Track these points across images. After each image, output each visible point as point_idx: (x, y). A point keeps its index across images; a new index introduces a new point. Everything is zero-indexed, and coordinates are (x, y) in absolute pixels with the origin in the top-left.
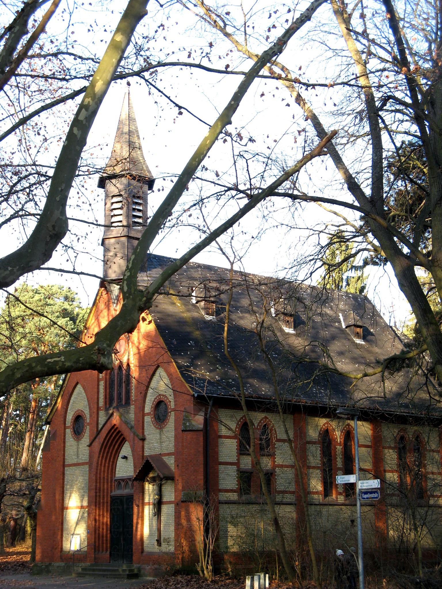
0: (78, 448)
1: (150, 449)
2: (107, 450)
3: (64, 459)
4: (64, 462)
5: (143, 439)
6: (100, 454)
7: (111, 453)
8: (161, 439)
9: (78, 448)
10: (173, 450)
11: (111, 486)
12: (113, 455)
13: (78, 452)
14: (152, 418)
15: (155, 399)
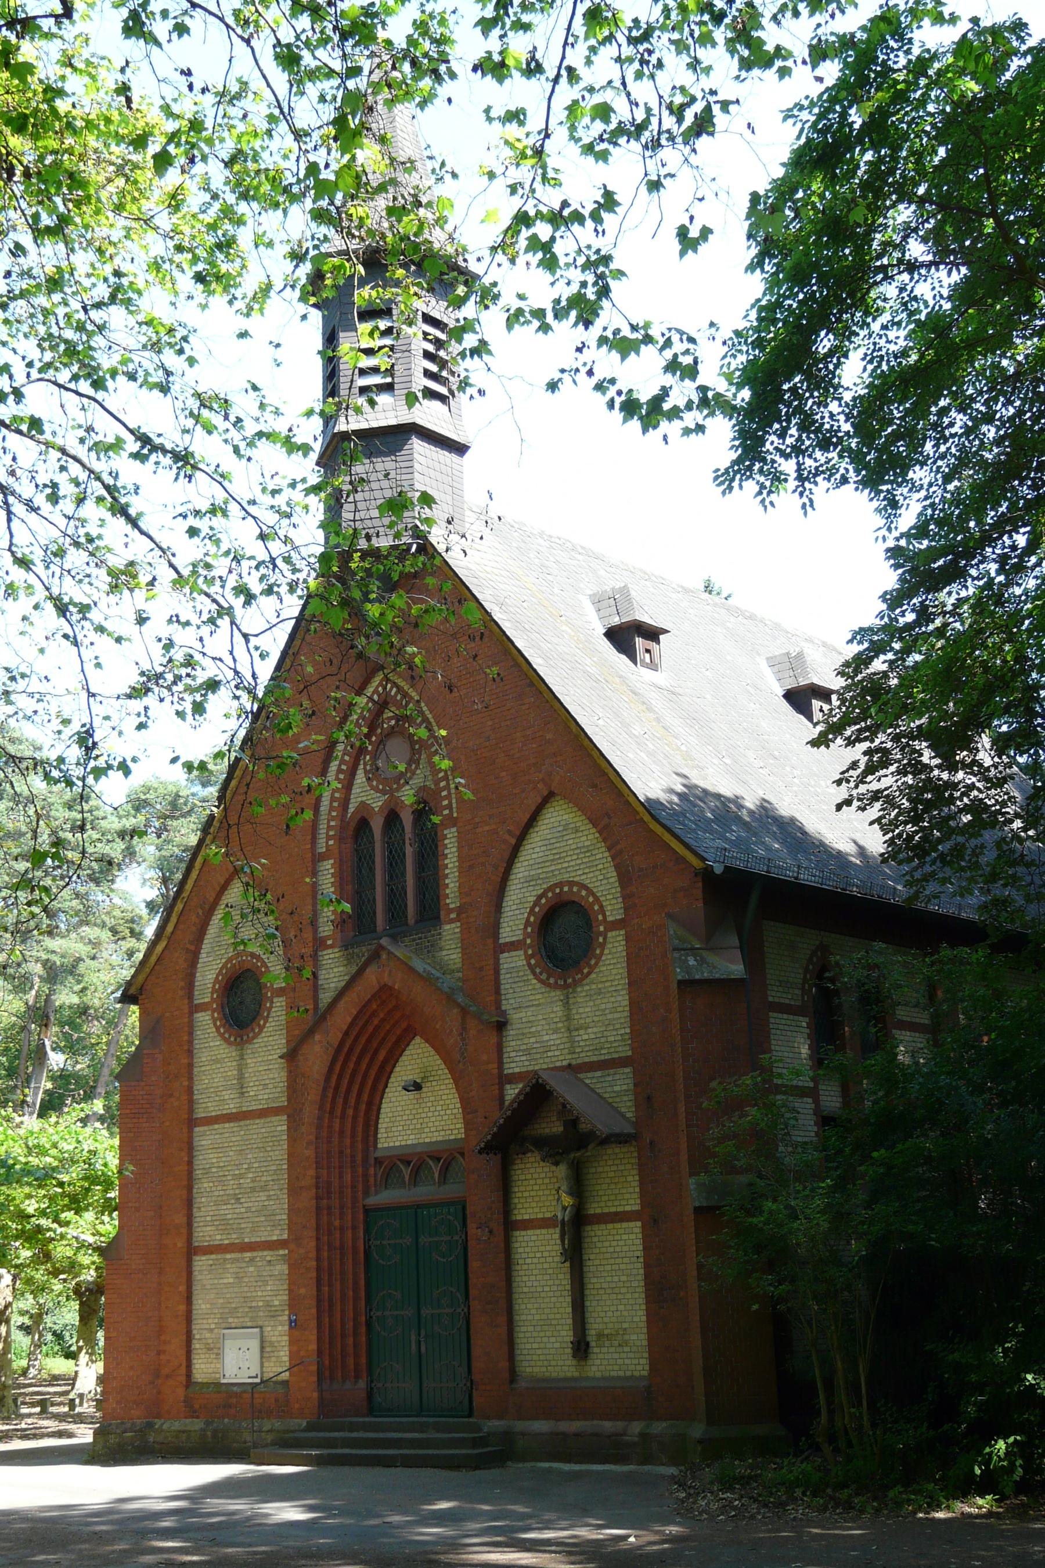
0: (241, 1068)
1: (528, 1052)
2: (351, 1065)
3: (191, 1102)
4: (191, 1110)
5: (501, 1026)
6: (327, 1079)
7: (365, 1076)
8: (568, 1018)
9: (241, 1068)
10: (625, 1051)
11: (365, 1175)
12: (370, 1082)
13: (241, 1077)
14: (528, 958)
15: (540, 897)
